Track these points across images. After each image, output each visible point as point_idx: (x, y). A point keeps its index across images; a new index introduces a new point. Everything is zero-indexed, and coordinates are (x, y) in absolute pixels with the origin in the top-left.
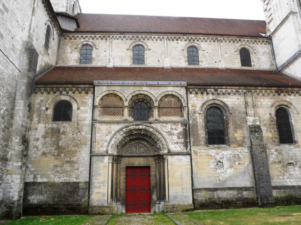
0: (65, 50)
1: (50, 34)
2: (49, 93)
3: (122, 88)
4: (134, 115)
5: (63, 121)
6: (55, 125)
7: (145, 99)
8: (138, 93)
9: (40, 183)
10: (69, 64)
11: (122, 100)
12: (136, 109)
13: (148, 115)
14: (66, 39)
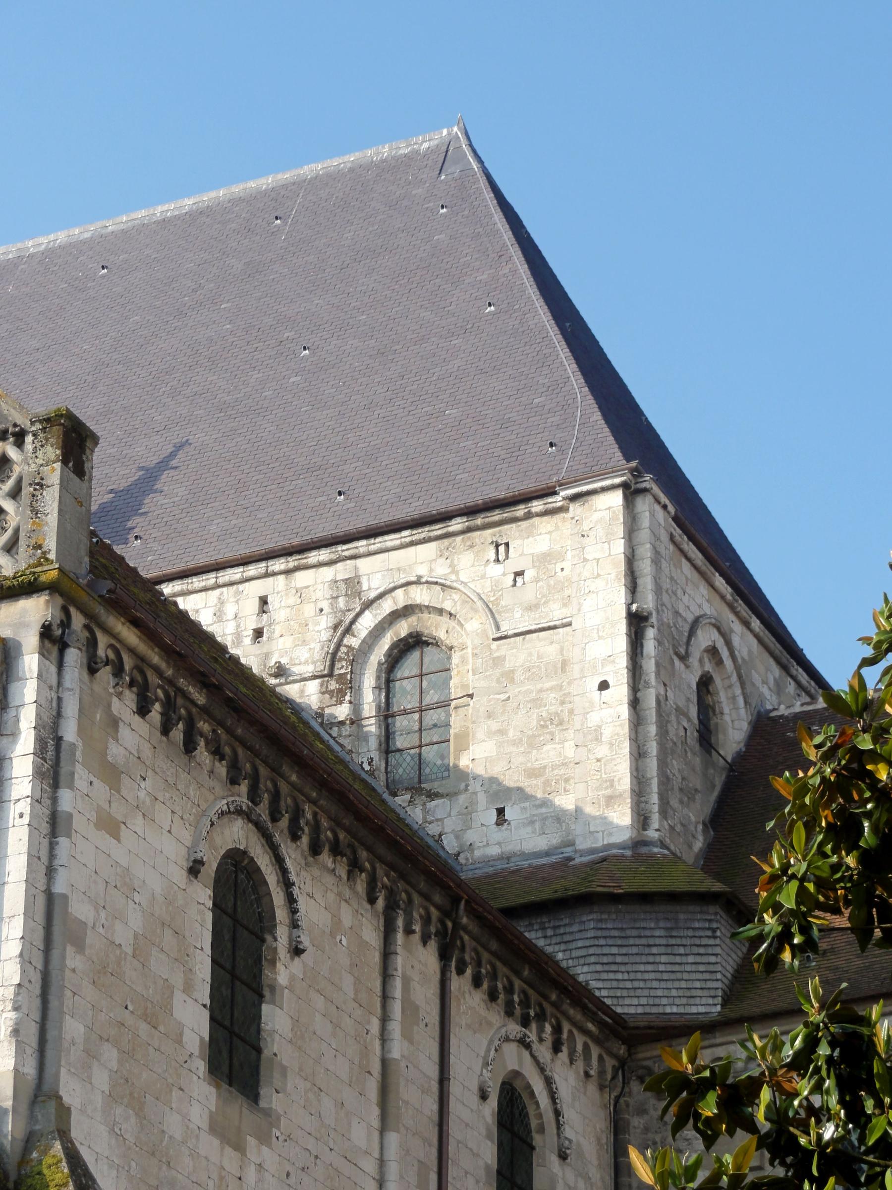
1: (534, 1123)
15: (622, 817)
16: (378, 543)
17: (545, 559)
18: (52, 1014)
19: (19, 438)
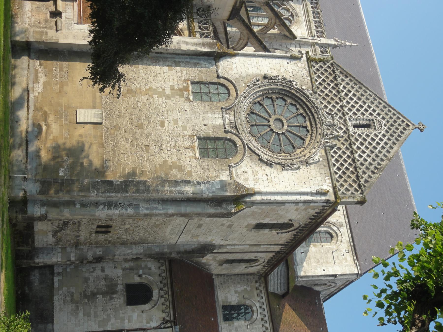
0: (239, 283)
1: (251, 263)
2: (160, 275)
5: (127, 296)
6: (120, 287)
9: (53, 280)
10: (218, 292)
14: (256, 282)
15: (302, 274)
16: (349, 230)
17: (346, 259)
18: (266, 204)
19: (361, 194)
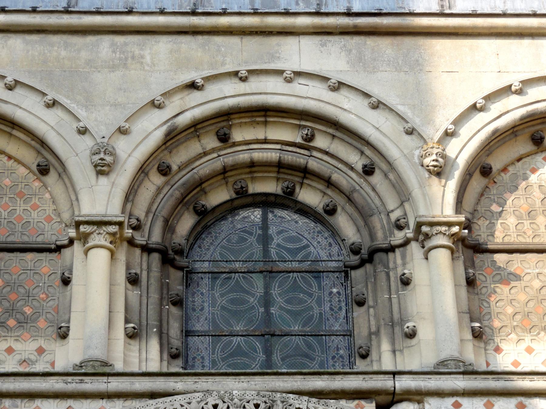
3: (58, 48)
4: (187, 333)
7: (305, 172)
8: (228, 94)
11: (51, 179)
12: (206, 280)
13: (349, 334)
